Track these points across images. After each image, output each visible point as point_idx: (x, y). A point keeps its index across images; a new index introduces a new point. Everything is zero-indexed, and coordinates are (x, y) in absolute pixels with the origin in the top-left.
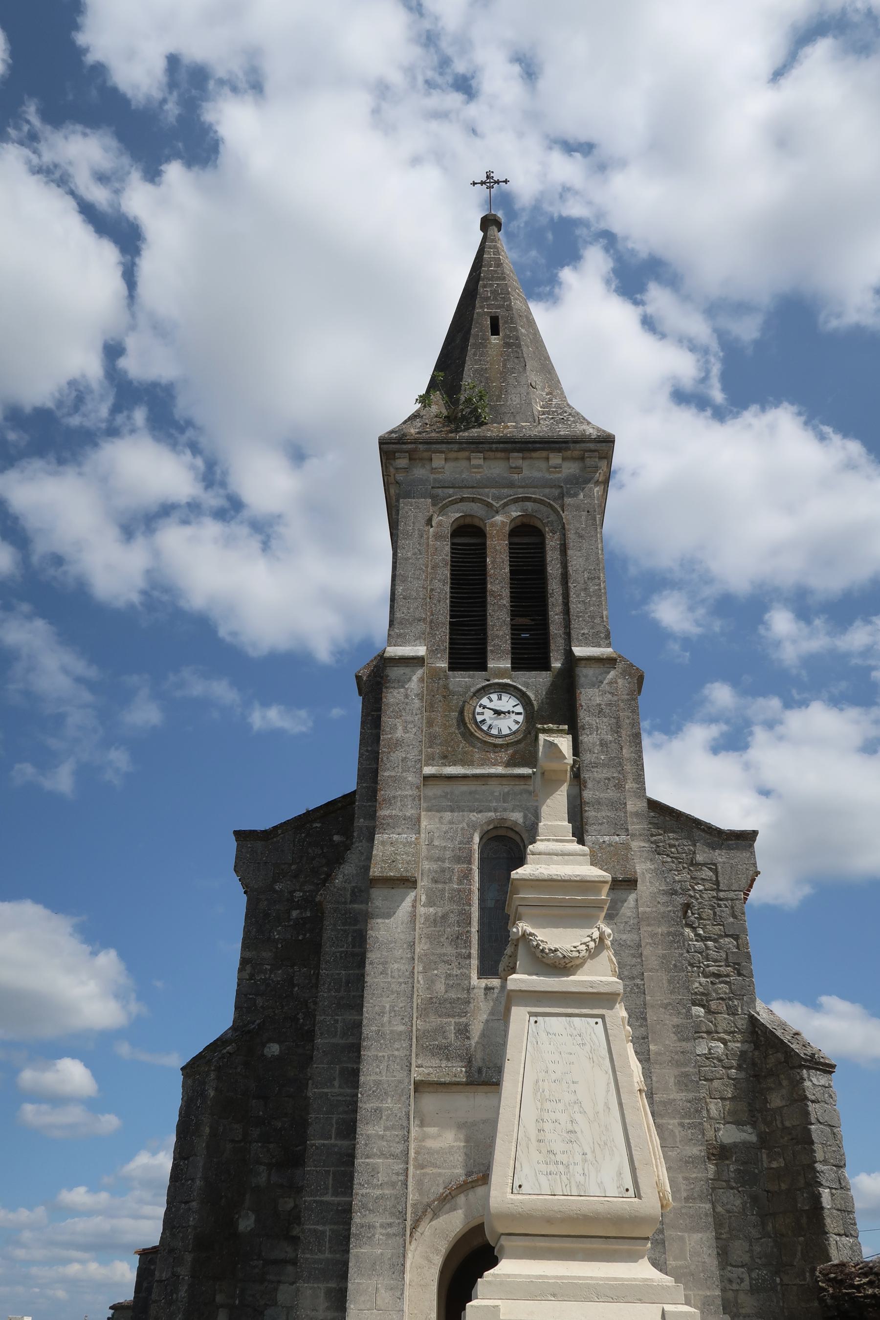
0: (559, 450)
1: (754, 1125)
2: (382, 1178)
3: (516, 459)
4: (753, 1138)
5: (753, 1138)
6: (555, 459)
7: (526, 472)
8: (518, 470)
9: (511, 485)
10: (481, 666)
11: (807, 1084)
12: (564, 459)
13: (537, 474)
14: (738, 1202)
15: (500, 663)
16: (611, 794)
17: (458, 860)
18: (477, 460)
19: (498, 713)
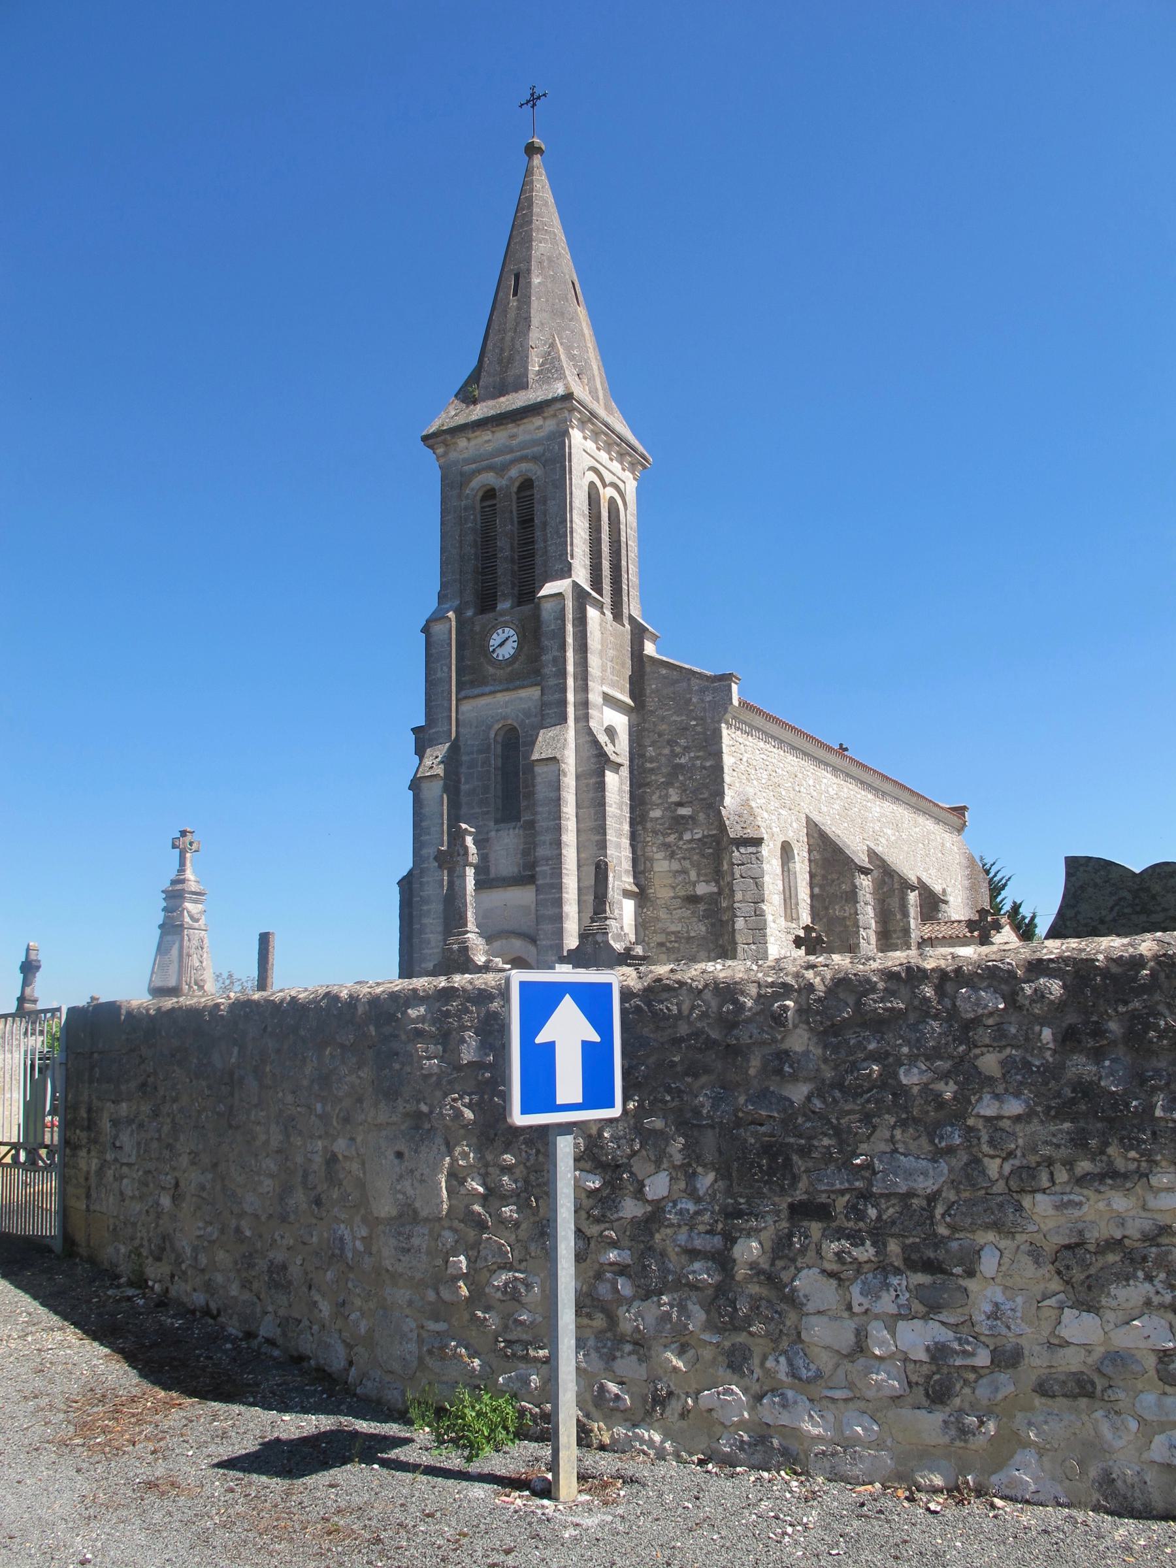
0: (539, 414)
1: (717, 882)
2: (433, 944)
3: (512, 429)
4: (715, 890)
5: (715, 890)
6: (538, 421)
7: (521, 438)
8: (513, 437)
9: (512, 451)
10: (493, 607)
11: (736, 854)
12: (545, 418)
13: (528, 437)
14: (704, 929)
15: (504, 605)
16: (557, 696)
17: (480, 752)
18: (486, 436)
19: (501, 645)
